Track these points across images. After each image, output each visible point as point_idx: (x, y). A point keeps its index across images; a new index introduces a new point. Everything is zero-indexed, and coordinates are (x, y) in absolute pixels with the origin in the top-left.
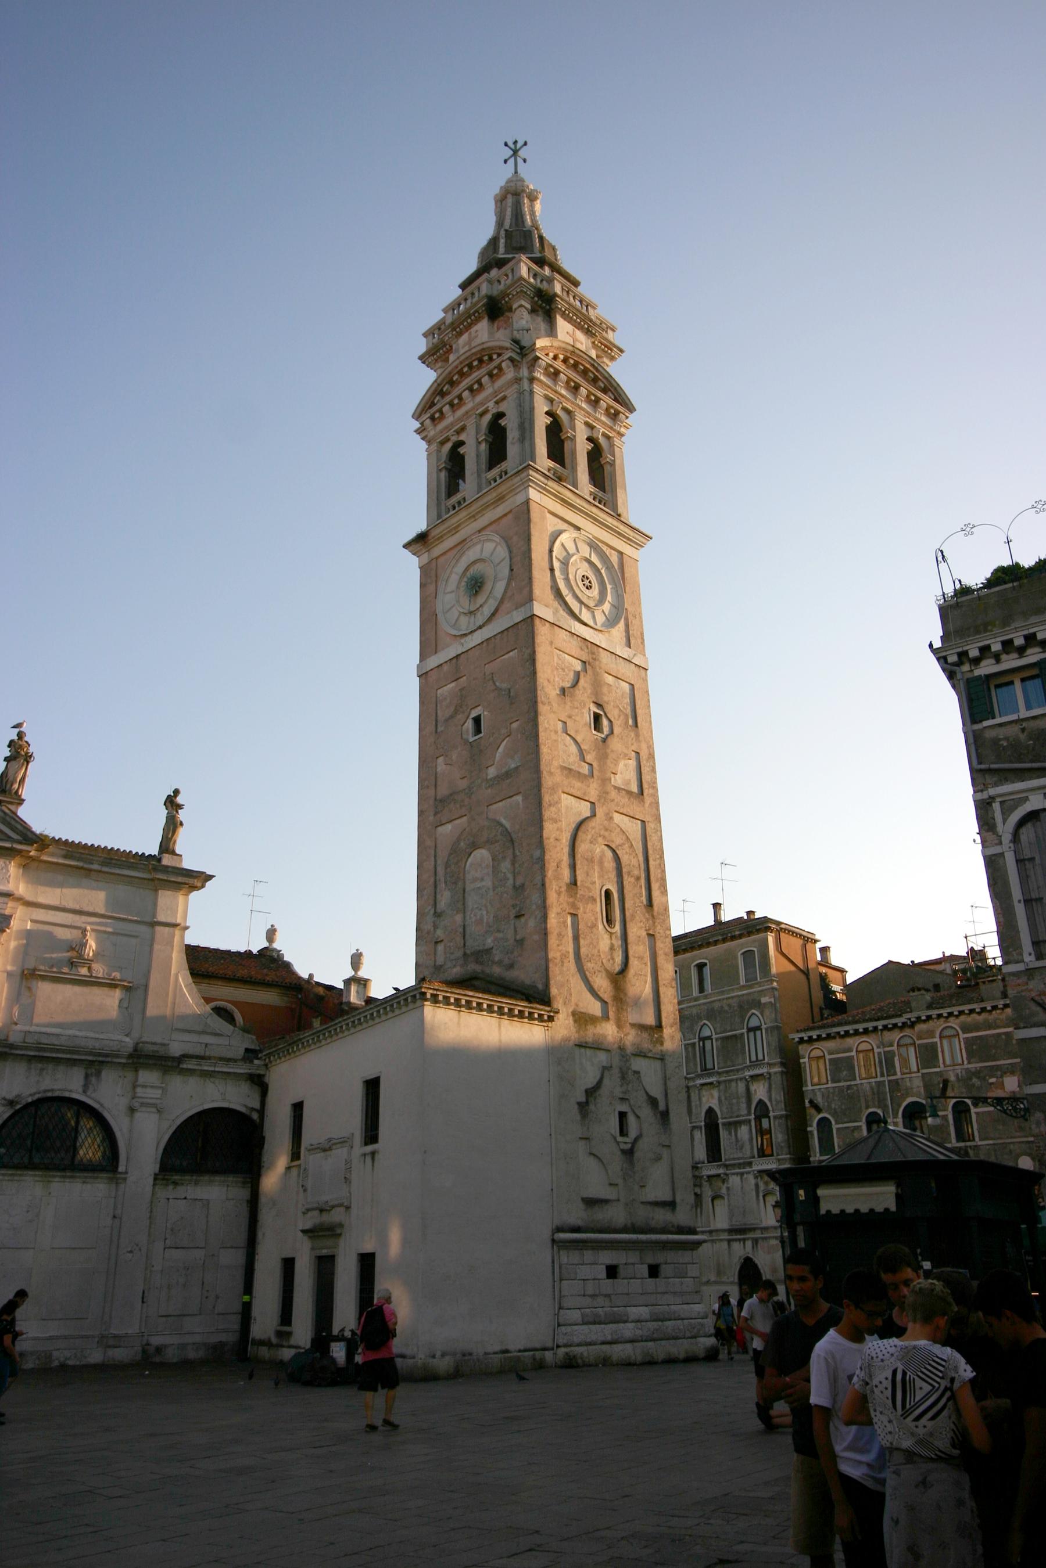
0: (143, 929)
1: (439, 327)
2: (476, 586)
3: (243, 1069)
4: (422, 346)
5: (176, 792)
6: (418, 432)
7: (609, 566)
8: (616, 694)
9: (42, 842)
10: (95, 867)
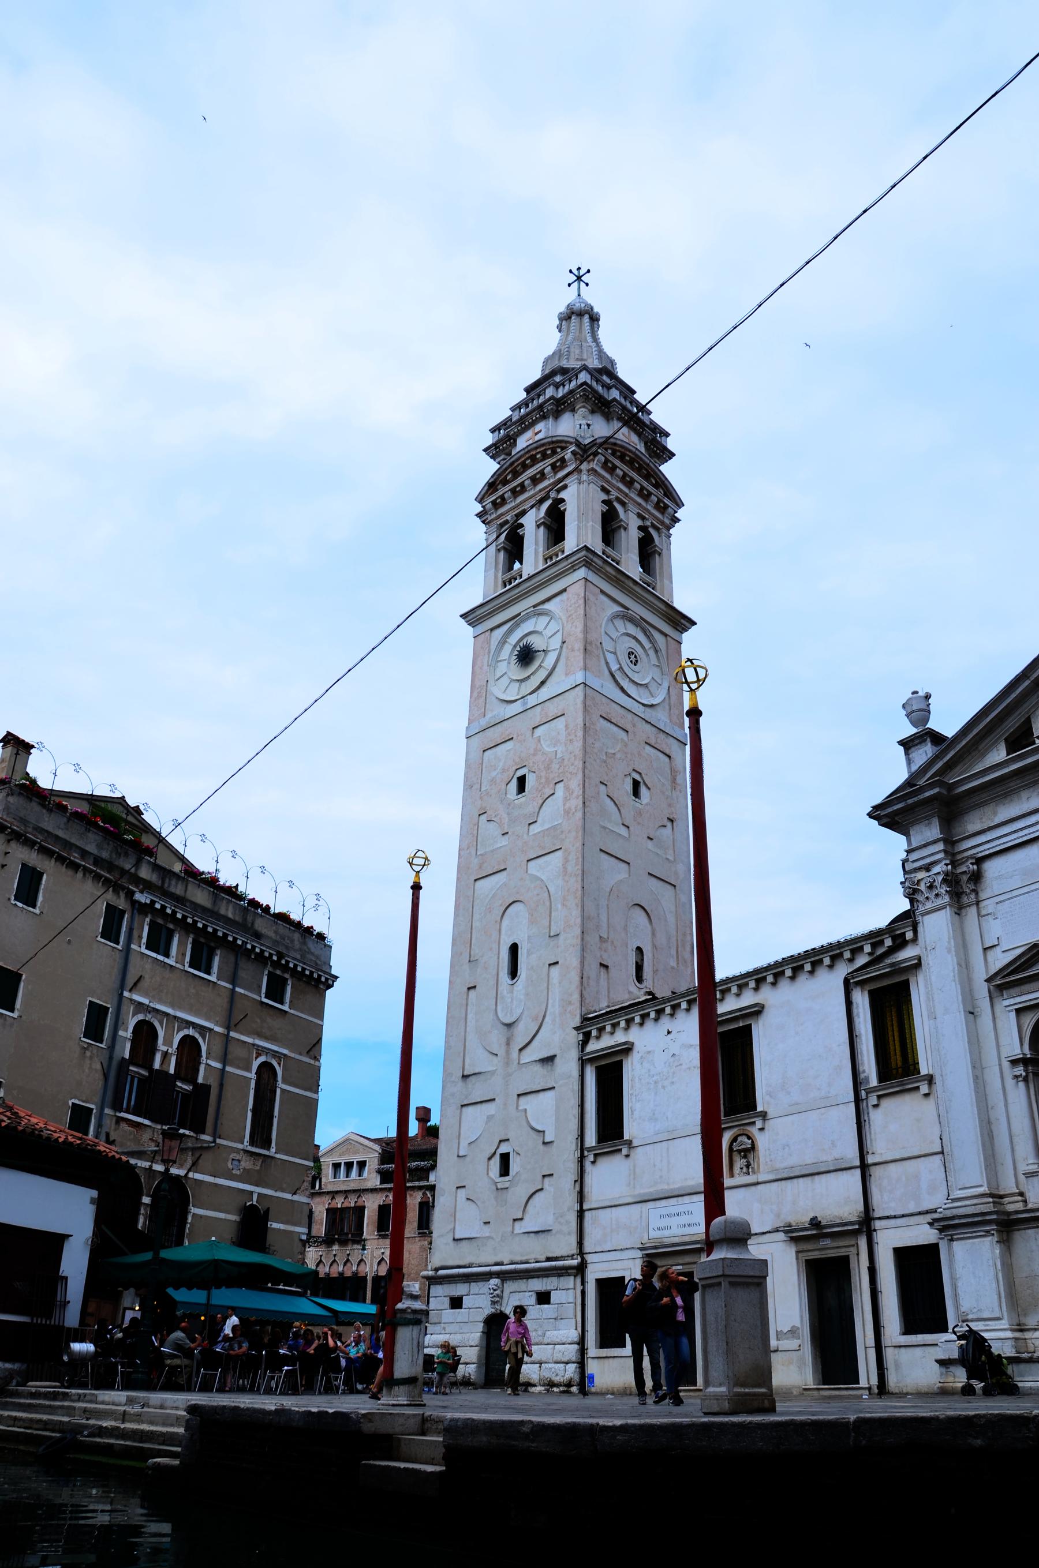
1: (505, 424)
4: (489, 439)
6: (479, 515)
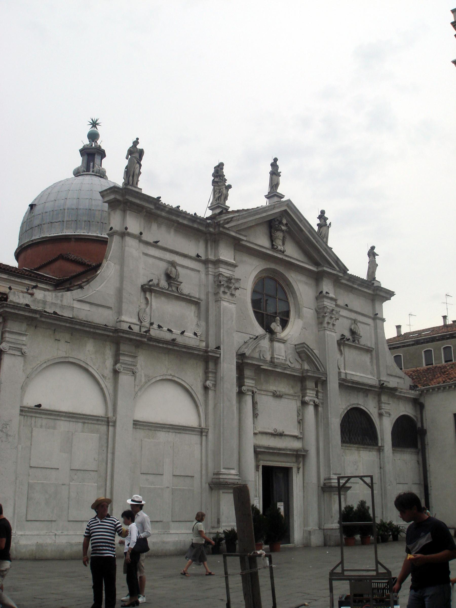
0: (370, 321)
5: (373, 248)
10: (356, 286)
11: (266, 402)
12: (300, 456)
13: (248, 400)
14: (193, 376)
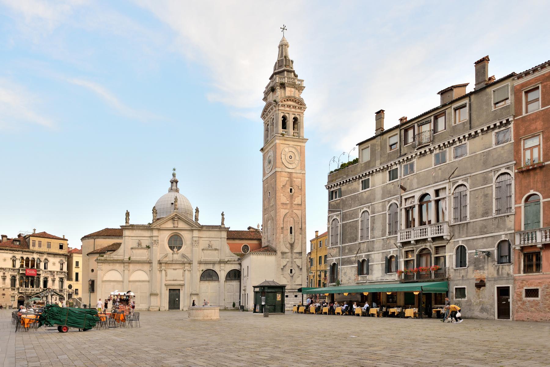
2: (270, 162)
3: (237, 262)
7: (297, 150)
8: (297, 181)
9: (203, 226)
11: (170, 272)
12: (183, 285)
13: (163, 272)
14: (146, 267)
